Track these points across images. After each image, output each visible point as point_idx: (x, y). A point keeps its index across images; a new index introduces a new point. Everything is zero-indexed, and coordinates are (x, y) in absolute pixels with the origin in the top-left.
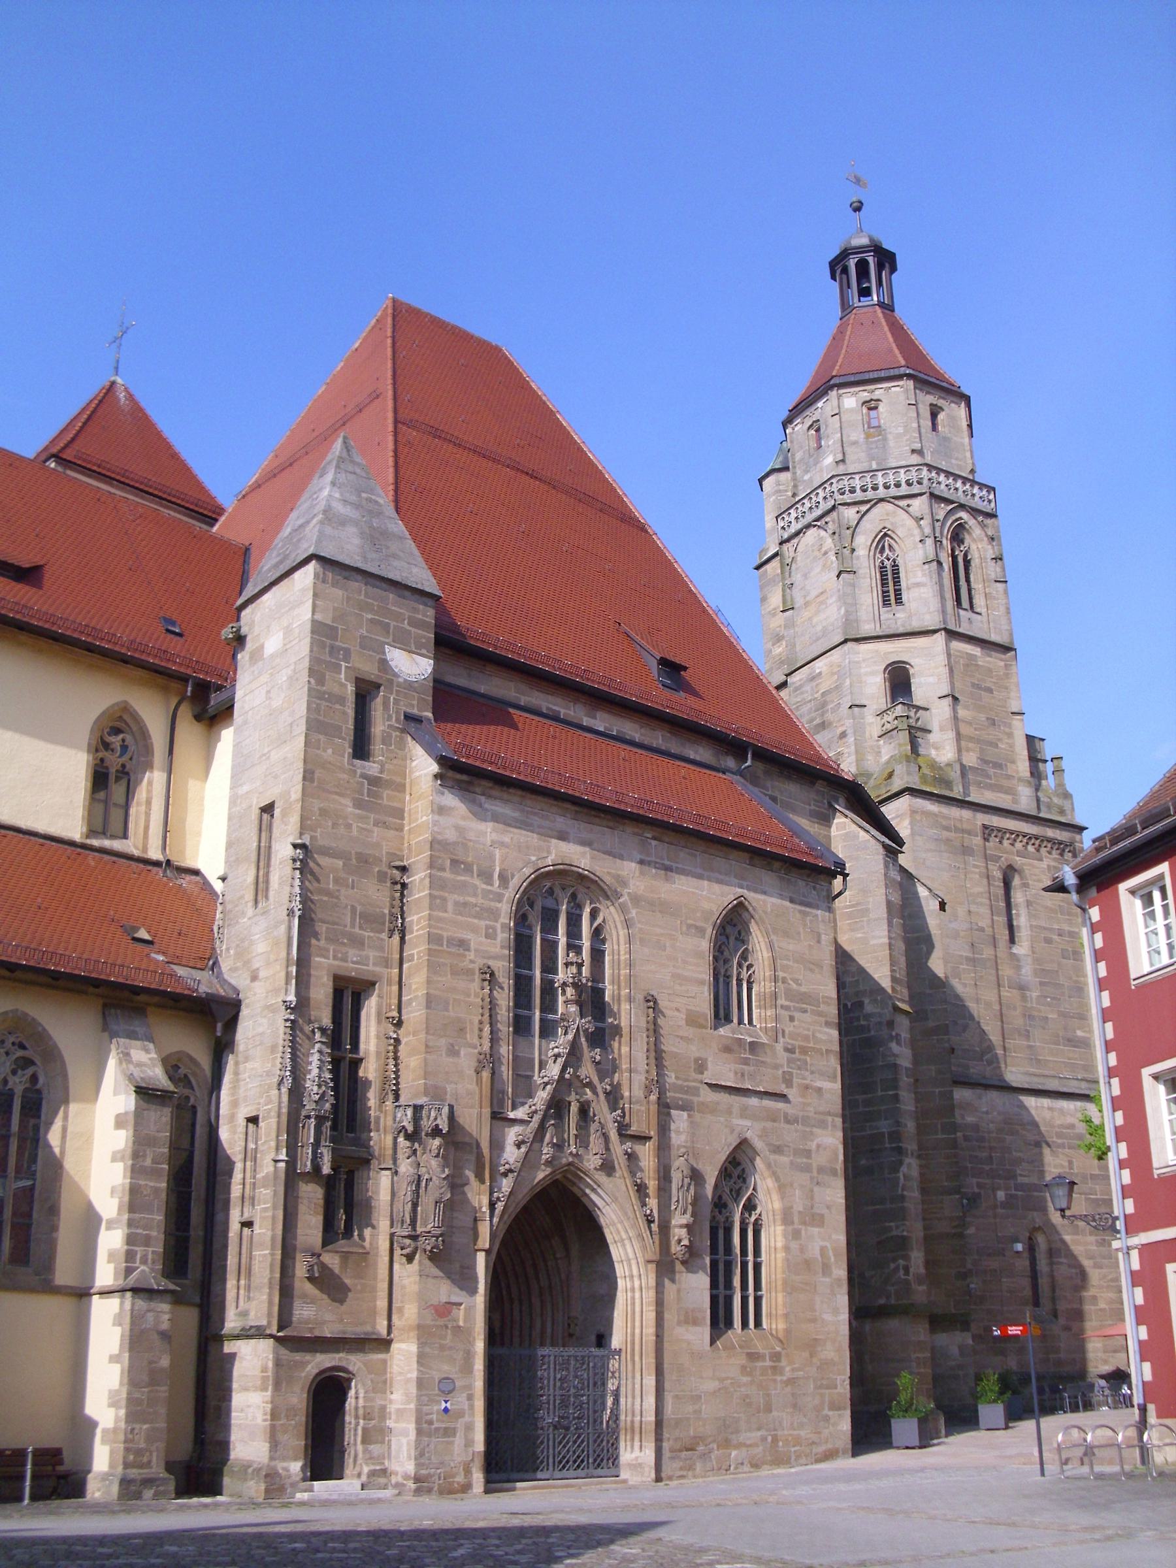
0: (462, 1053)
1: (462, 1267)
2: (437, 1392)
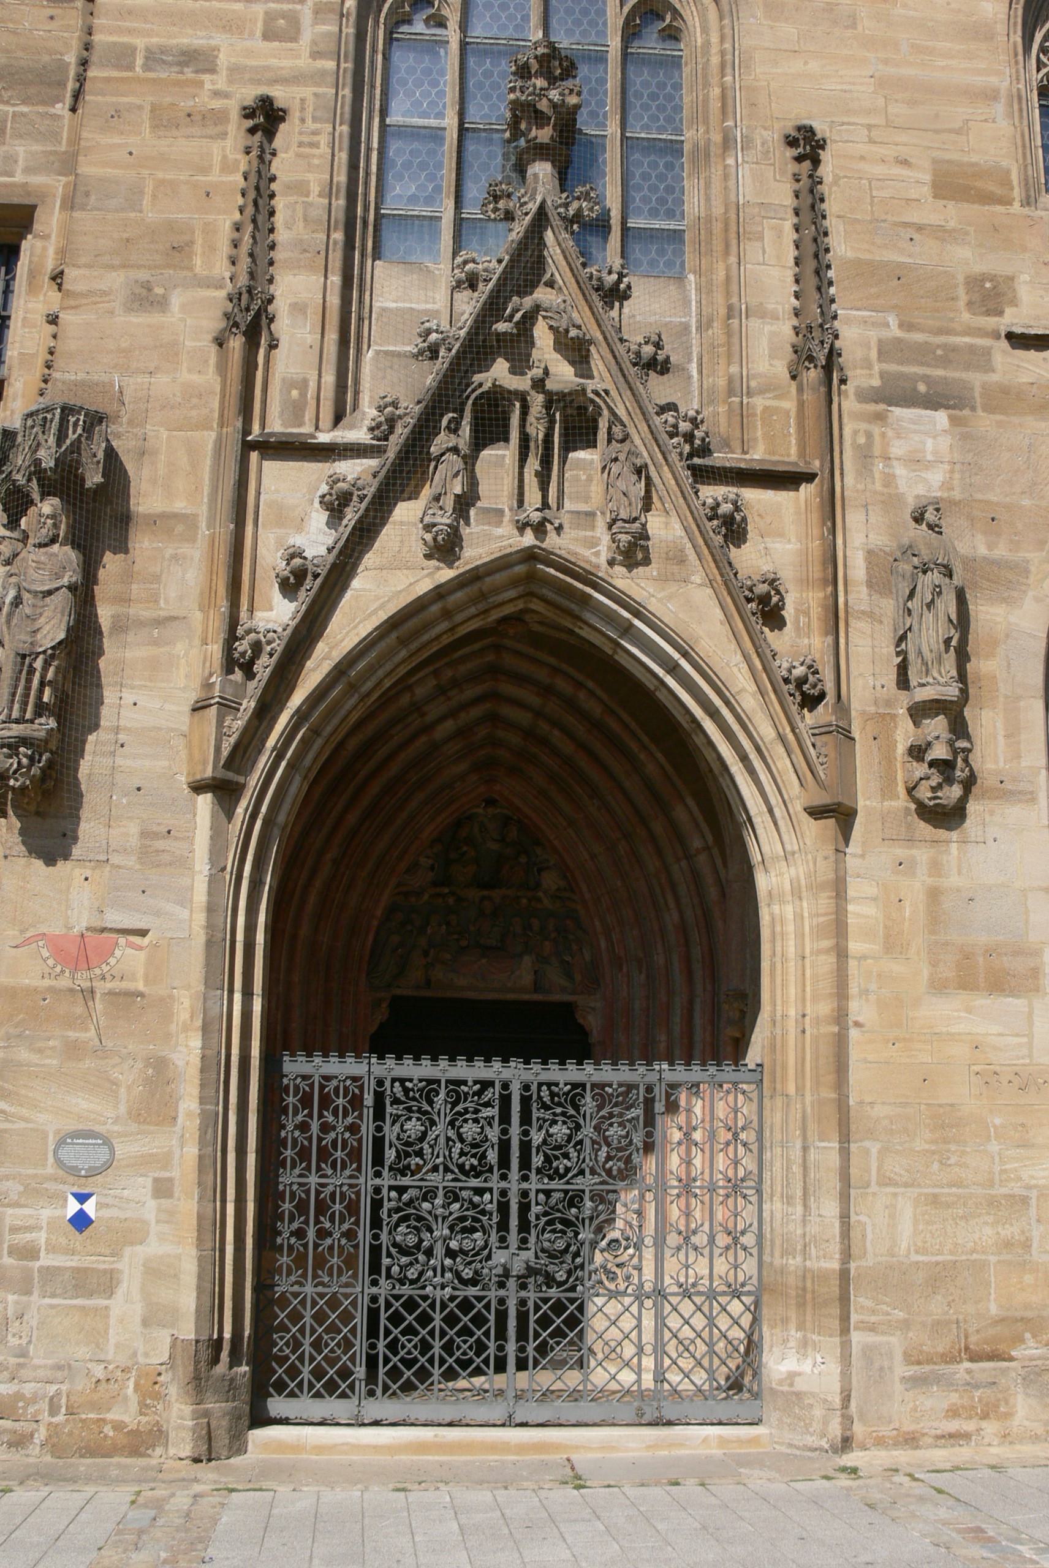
0: (177, 300)
1: (145, 834)
2: (50, 1168)
